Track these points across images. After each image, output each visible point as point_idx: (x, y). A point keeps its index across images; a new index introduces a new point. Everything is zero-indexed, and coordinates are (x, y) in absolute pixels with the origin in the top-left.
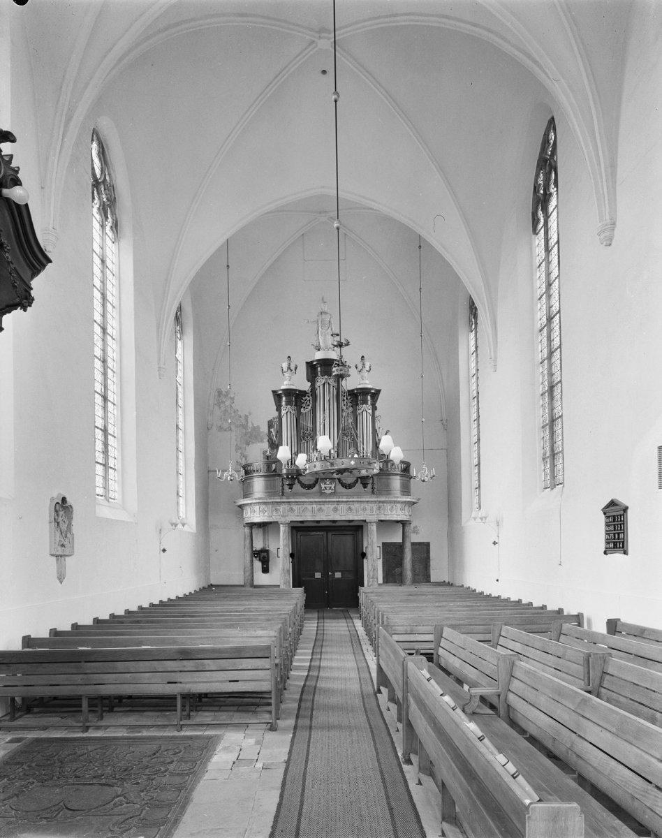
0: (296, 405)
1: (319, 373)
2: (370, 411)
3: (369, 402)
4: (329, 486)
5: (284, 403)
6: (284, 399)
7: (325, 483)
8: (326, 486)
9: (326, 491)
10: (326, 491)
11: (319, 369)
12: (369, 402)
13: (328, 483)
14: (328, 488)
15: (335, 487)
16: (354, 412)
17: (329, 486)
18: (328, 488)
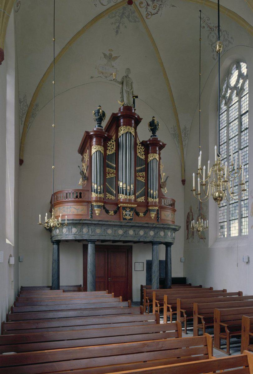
0: (104, 146)
1: (122, 124)
2: (158, 159)
3: (158, 152)
4: (129, 213)
5: (94, 143)
6: (94, 140)
7: (126, 211)
8: (127, 213)
9: (126, 217)
10: (126, 217)
11: (122, 121)
12: (158, 152)
13: (128, 211)
14: (128, 215)
15: (133, 214)
16: (147, 158)
17: (129, 213)
18: (128, 215)
